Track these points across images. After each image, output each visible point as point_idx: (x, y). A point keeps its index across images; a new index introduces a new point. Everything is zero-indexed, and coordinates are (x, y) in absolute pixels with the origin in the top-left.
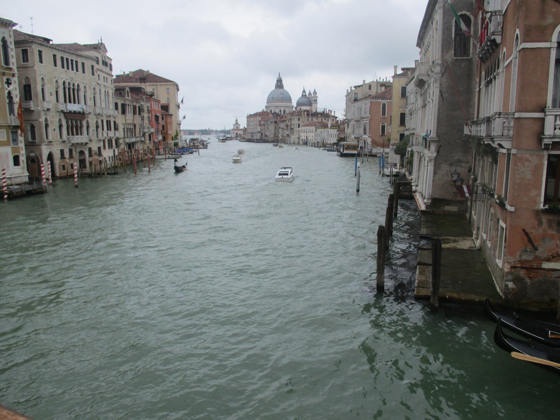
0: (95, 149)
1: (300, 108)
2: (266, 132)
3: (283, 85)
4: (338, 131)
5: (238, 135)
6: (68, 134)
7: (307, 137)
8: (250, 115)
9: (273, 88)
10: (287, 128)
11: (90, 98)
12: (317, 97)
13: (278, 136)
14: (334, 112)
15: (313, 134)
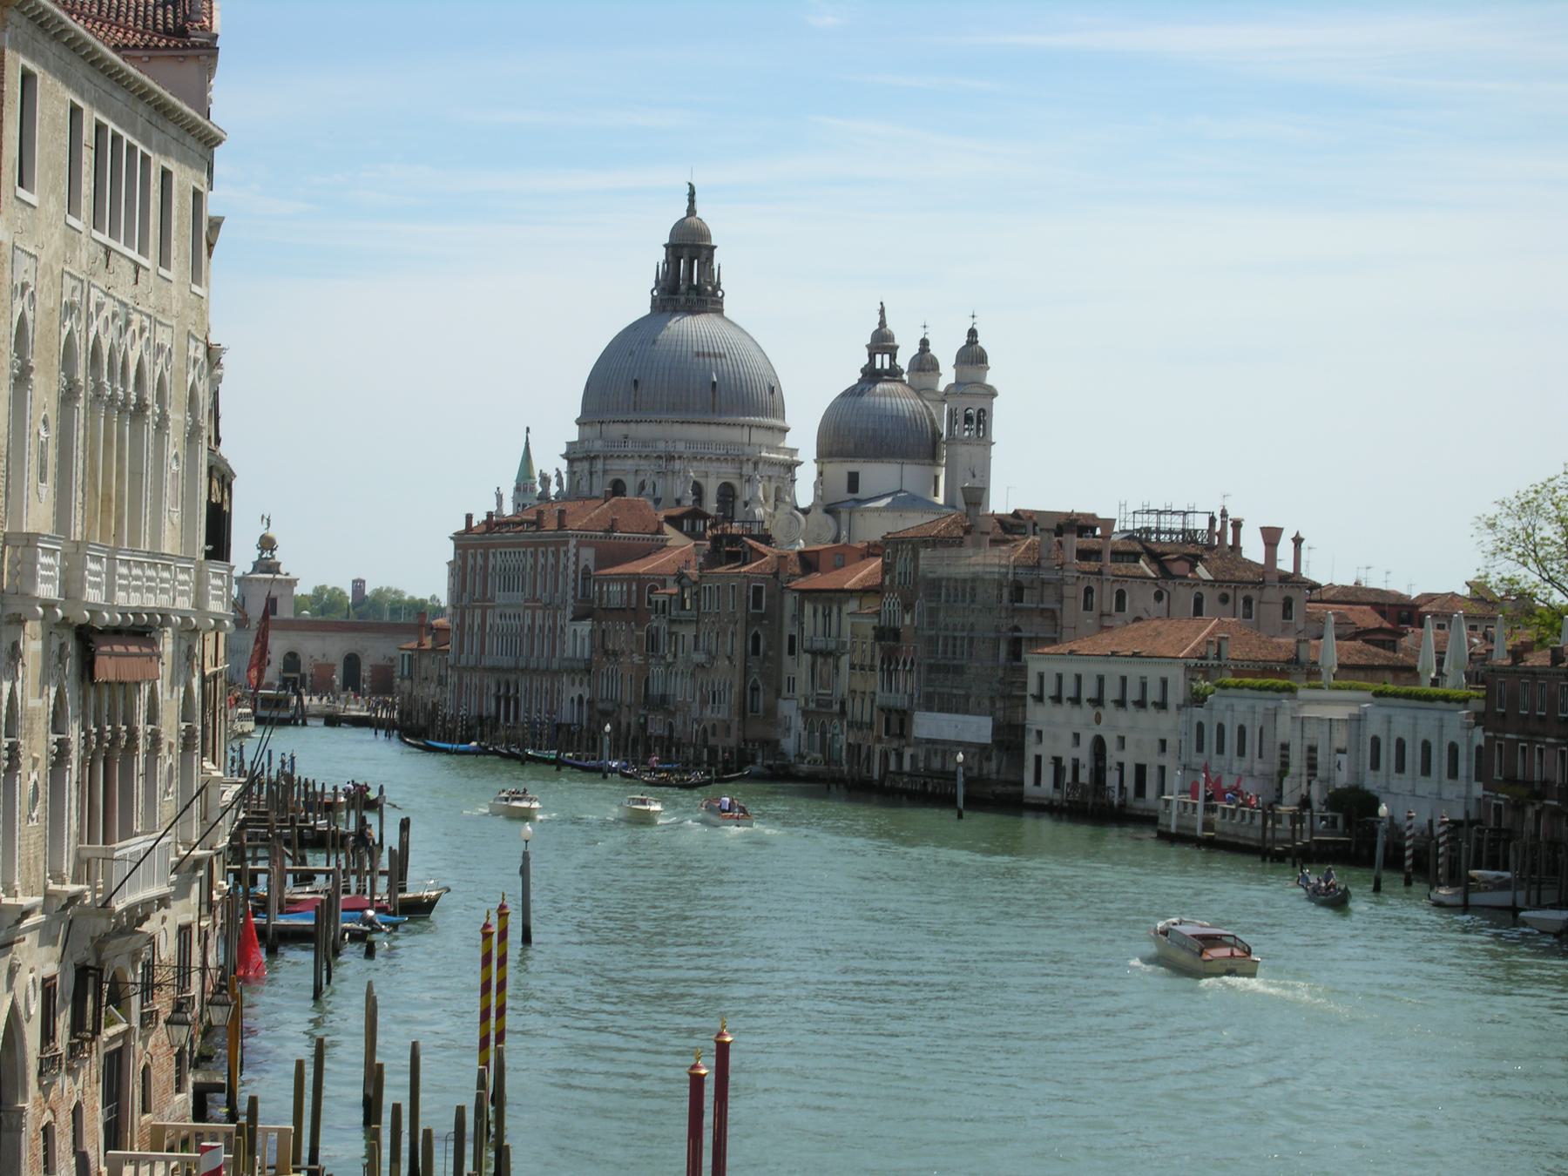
0: (167, 950)
1: (853, 481)
2: (657, 670)
3: (717, 287)
4: (1480, 719)
5: (306, 668)
6: (81, 841)
7: (1099, 745)
8: (493, 523)
9: (641, 306)
10: (890, 658)
11: (175, 475)
12: (992, 393)
13: (771, 712)
14: (1298, 541)
15: (1169, 724)
